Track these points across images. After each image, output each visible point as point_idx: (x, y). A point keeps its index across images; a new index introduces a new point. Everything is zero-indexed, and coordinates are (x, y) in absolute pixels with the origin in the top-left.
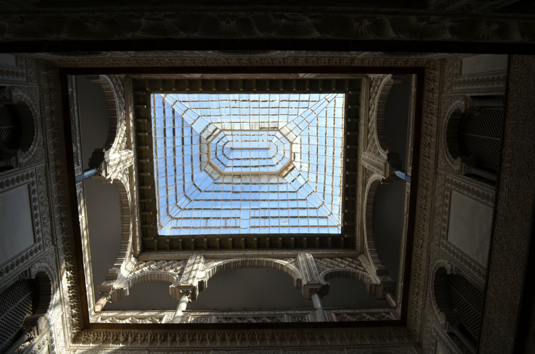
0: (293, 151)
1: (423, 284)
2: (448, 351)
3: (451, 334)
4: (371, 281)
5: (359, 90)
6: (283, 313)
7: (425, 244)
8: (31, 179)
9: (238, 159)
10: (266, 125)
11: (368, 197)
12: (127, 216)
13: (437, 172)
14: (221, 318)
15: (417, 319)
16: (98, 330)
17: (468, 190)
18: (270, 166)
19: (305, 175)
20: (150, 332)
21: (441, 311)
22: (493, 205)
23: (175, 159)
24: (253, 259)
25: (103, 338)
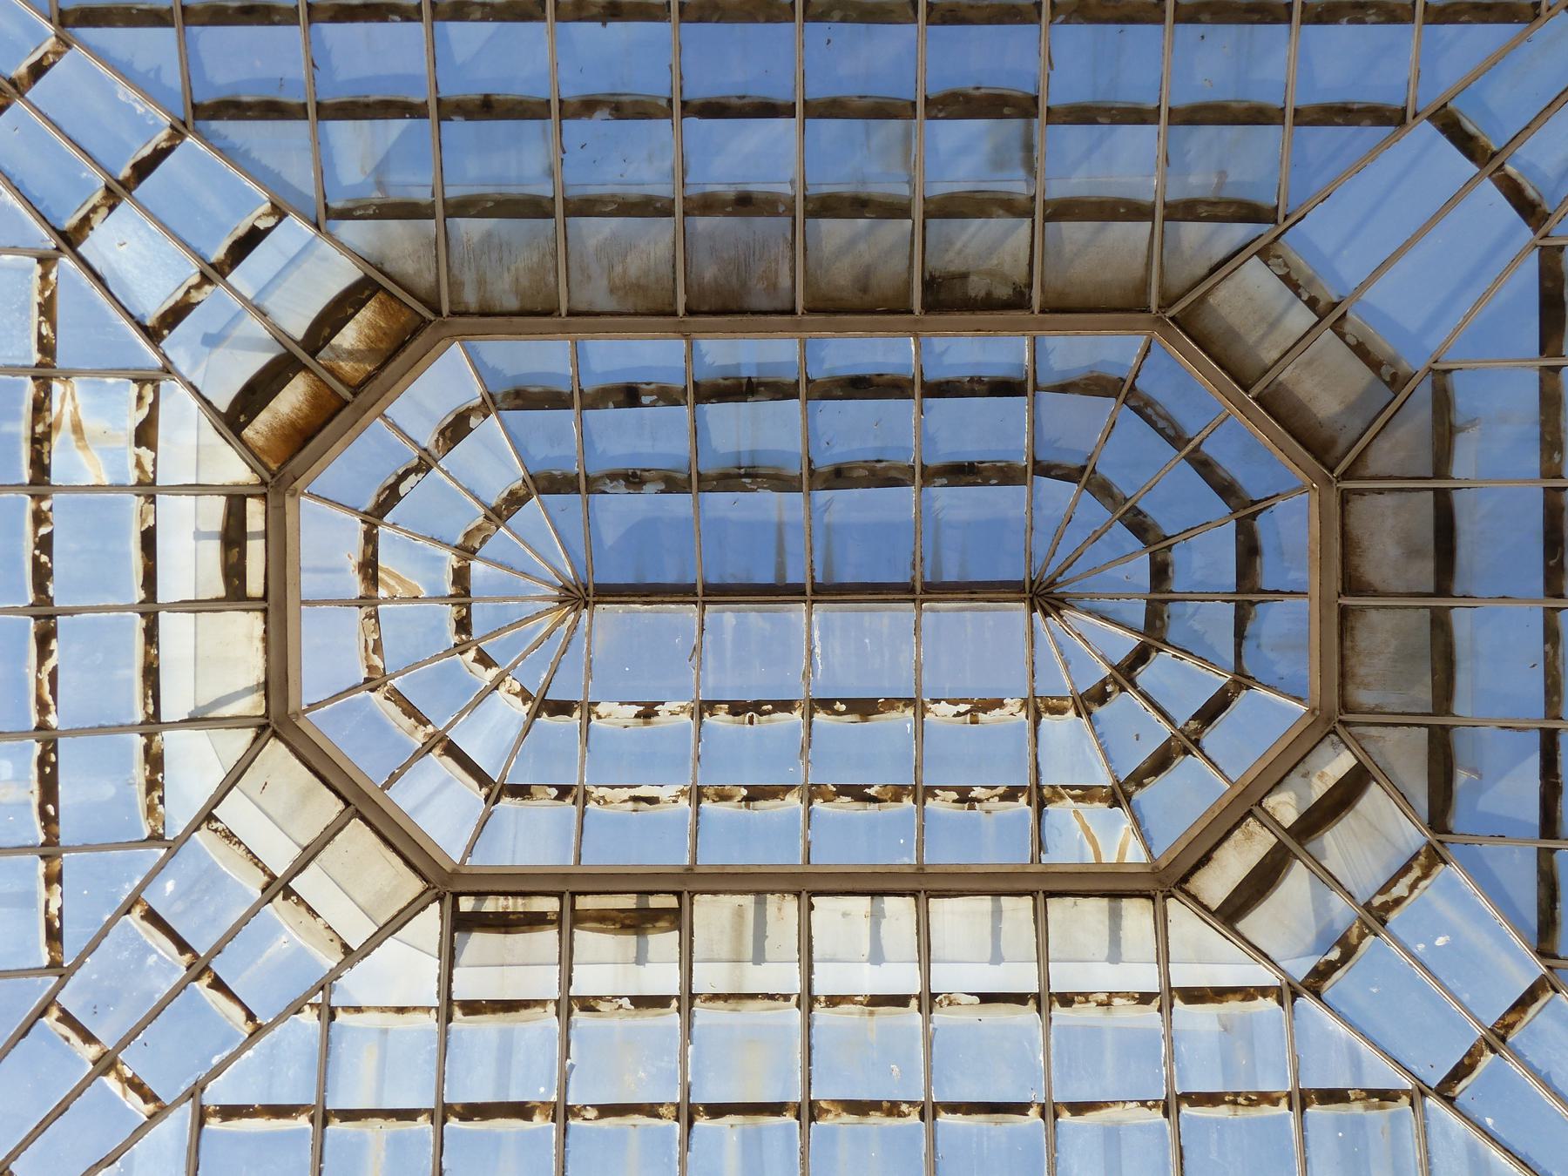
0: (249, 625)
10: (603, 963)
18: (557, 401)
19: (86, 324)
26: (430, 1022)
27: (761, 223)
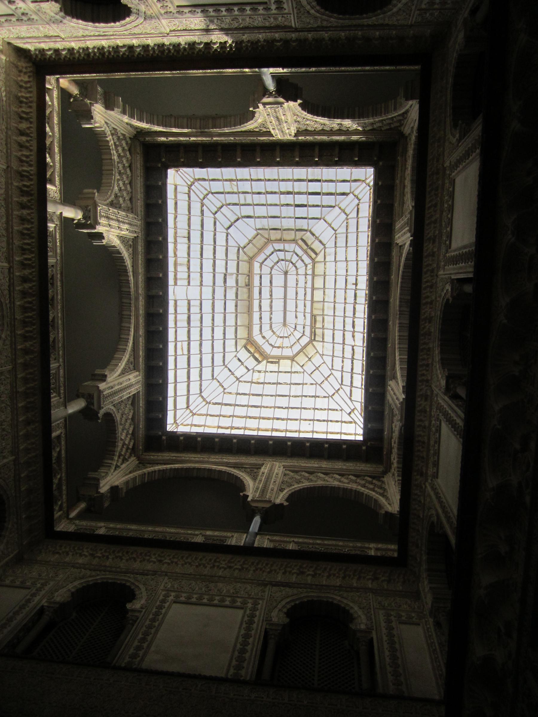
0: (281, 361)
1: (108, 564)
2: (17, 608)
4: (104, 477)
5: (367, 460)
6: (61, 360)
7: (164, 568)
8: (273, 7)
9: (271, 282)
10: (319, 325)
11: (220, 472)
12: (198, 125)
13: (266, 585)
14: (52, 271)
15: (57, 556)
16: (34, 89)
17: (247, 636)
19: (248, 377)
20: (33, 169)
22: (229, 677)
23: (275, 193)
24: (133, 309)
25: (22, 97)
26: (325, 343)
27: (238, 304)
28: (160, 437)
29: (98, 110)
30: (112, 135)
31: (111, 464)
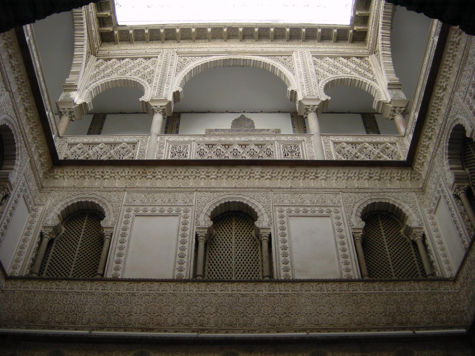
1: (437, 132)
3: (457, 197)
6: (273, 139)
15: (425, 164)
21: (451, 169)
28: (354, 31)
29: (78, 98)
30: (96, 81)
31: (369, 85)
